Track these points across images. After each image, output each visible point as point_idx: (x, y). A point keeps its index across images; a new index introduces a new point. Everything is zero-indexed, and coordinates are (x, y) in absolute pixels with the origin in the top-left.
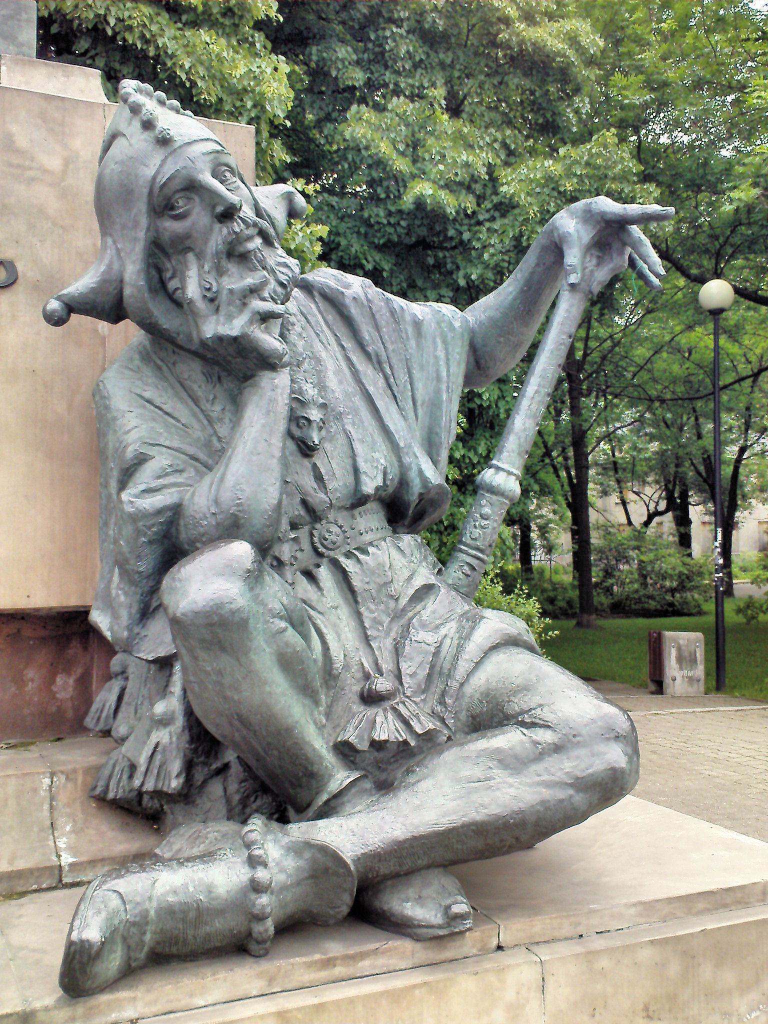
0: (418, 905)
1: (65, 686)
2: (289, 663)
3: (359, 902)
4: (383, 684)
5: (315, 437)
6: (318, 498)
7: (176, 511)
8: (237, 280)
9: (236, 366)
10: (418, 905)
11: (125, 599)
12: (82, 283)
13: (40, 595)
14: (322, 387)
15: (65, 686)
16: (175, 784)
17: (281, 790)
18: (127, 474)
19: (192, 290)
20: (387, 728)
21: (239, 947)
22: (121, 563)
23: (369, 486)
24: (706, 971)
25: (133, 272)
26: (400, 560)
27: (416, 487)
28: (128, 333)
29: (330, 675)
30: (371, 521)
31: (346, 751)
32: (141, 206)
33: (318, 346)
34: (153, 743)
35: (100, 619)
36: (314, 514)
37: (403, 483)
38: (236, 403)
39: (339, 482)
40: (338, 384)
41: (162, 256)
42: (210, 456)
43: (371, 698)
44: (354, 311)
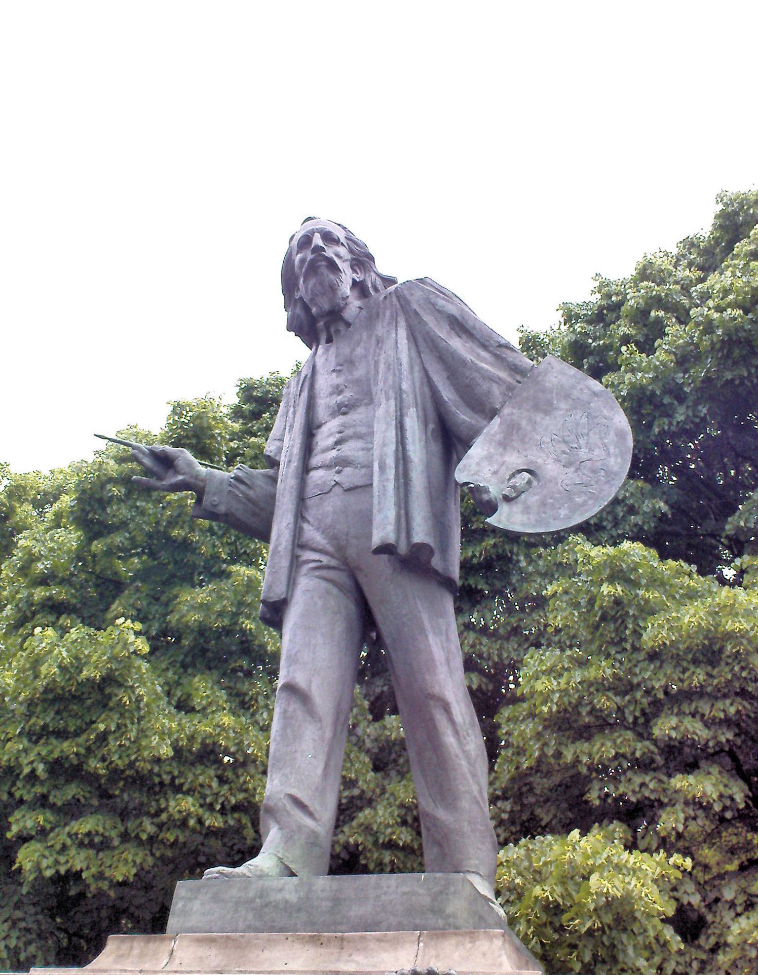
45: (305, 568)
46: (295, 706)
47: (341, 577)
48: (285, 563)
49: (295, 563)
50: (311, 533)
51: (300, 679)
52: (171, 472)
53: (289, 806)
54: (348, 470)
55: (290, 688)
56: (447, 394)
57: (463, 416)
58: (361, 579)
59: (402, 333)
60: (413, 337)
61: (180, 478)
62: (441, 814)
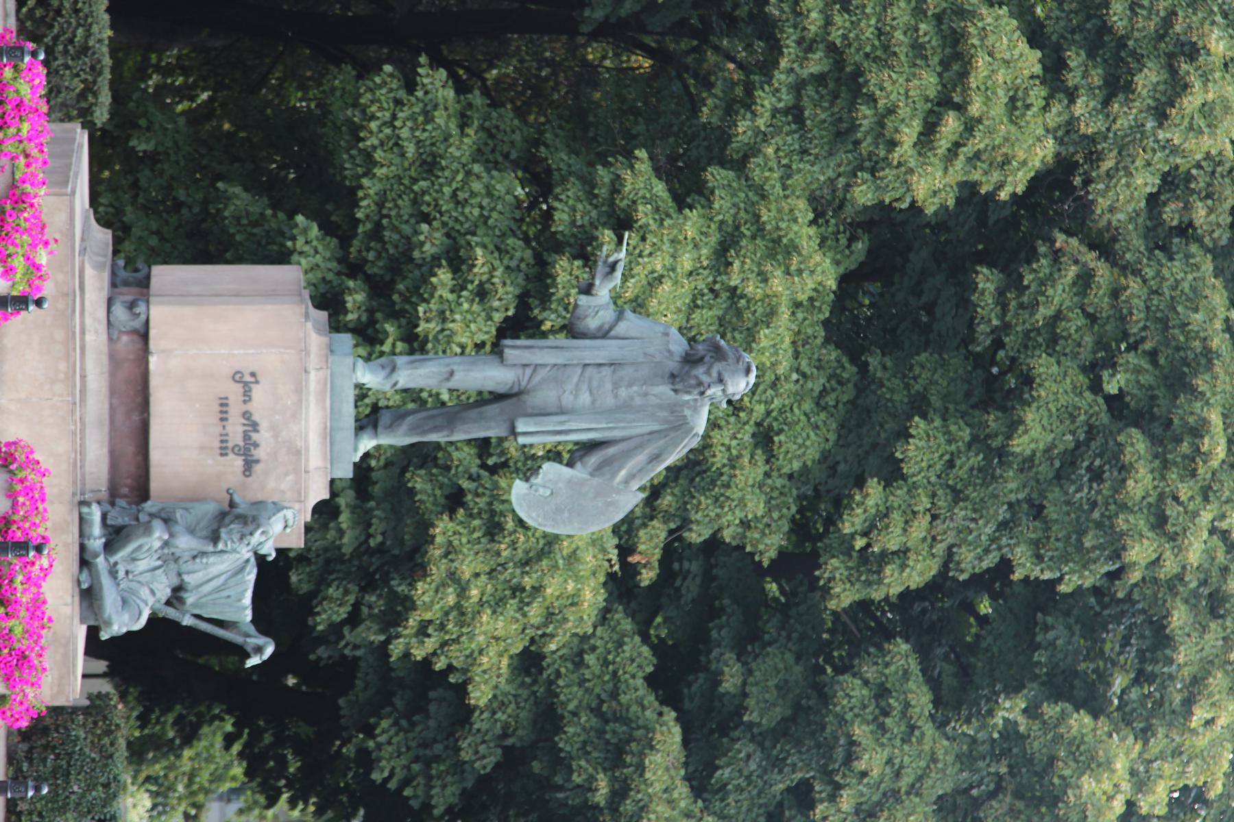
0: (84, 576)
1: (125, 490)
2: (140, 546)
3: (85, 562)
4: (130, 576)
5: (198, 560)
6: (181, 561)
7: (176, 522)
8: (236, 537)
9: (215, 538)
10: (84, 576)
11: (154, 510)
12: (237, 499)
13: (154, 486)
14: (214, 564)
15: (125, 490)
16: (109, 522)
17: (109, 547)
18: (186, 509)
19: (232, 526)
20: (121, 574)
21: (81, 535)
22: (163, 509)
23: (186, 578)
24: (61, 651)
25: (238, 511)
26: (164, 592)
27: (185, 595)
28: (227, 509)
29: (134, 560)
30: (175, 582)
31: (116, 564)
32: (255, 513)
33: (226, 564)
34: (116, 519)
35: (149, 503)
36: (176, 560)
37: (186, 591)
38: (206, 538)
39: (185, 568)
40: (214, 570)
41: (243, 519)
42: (191, 531)
43: (127, 573)
44: (240, 576)
45: (520, 371)
46: (446, 376)
47: (516, 389)
48: (525, 362)
49: (525, 365)
50: (542, 373)
51: (457, 376)
52: (608, 269)
53: (393, 381)
54: (571, 397)
55: (452, 373)
56: (611, 451)
57: (594, 459)
58: (514, 399)
59: (656, 427)
60: (651, 433)
61: (597, 282)
62: (404, 427)
